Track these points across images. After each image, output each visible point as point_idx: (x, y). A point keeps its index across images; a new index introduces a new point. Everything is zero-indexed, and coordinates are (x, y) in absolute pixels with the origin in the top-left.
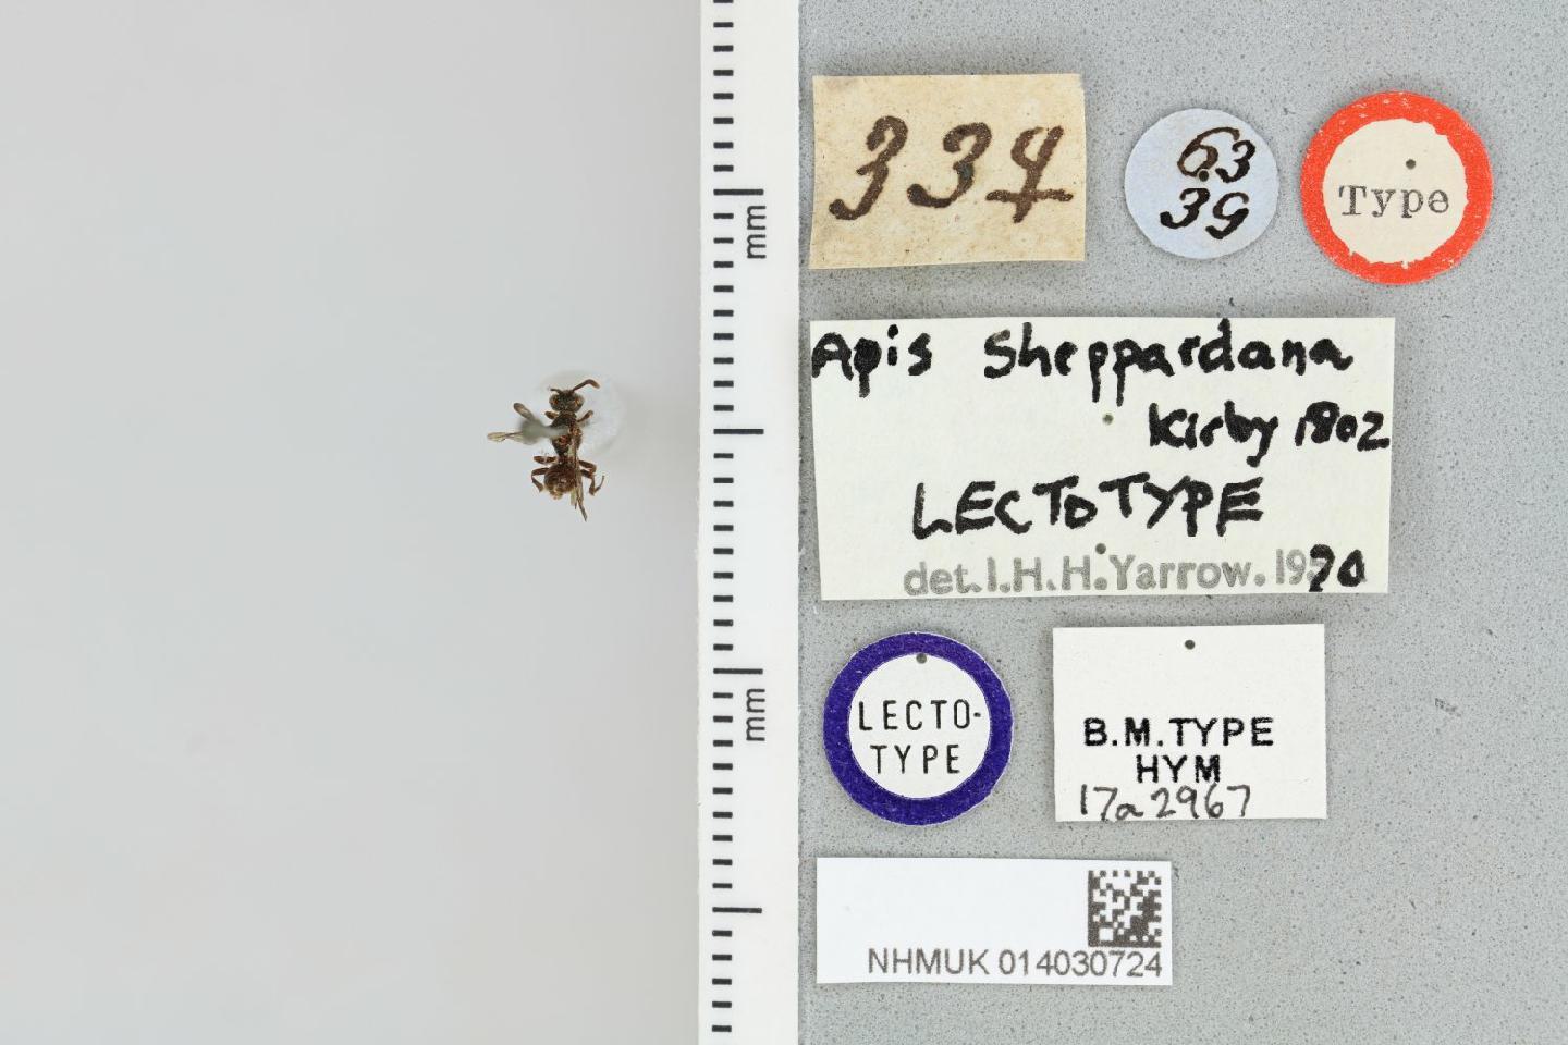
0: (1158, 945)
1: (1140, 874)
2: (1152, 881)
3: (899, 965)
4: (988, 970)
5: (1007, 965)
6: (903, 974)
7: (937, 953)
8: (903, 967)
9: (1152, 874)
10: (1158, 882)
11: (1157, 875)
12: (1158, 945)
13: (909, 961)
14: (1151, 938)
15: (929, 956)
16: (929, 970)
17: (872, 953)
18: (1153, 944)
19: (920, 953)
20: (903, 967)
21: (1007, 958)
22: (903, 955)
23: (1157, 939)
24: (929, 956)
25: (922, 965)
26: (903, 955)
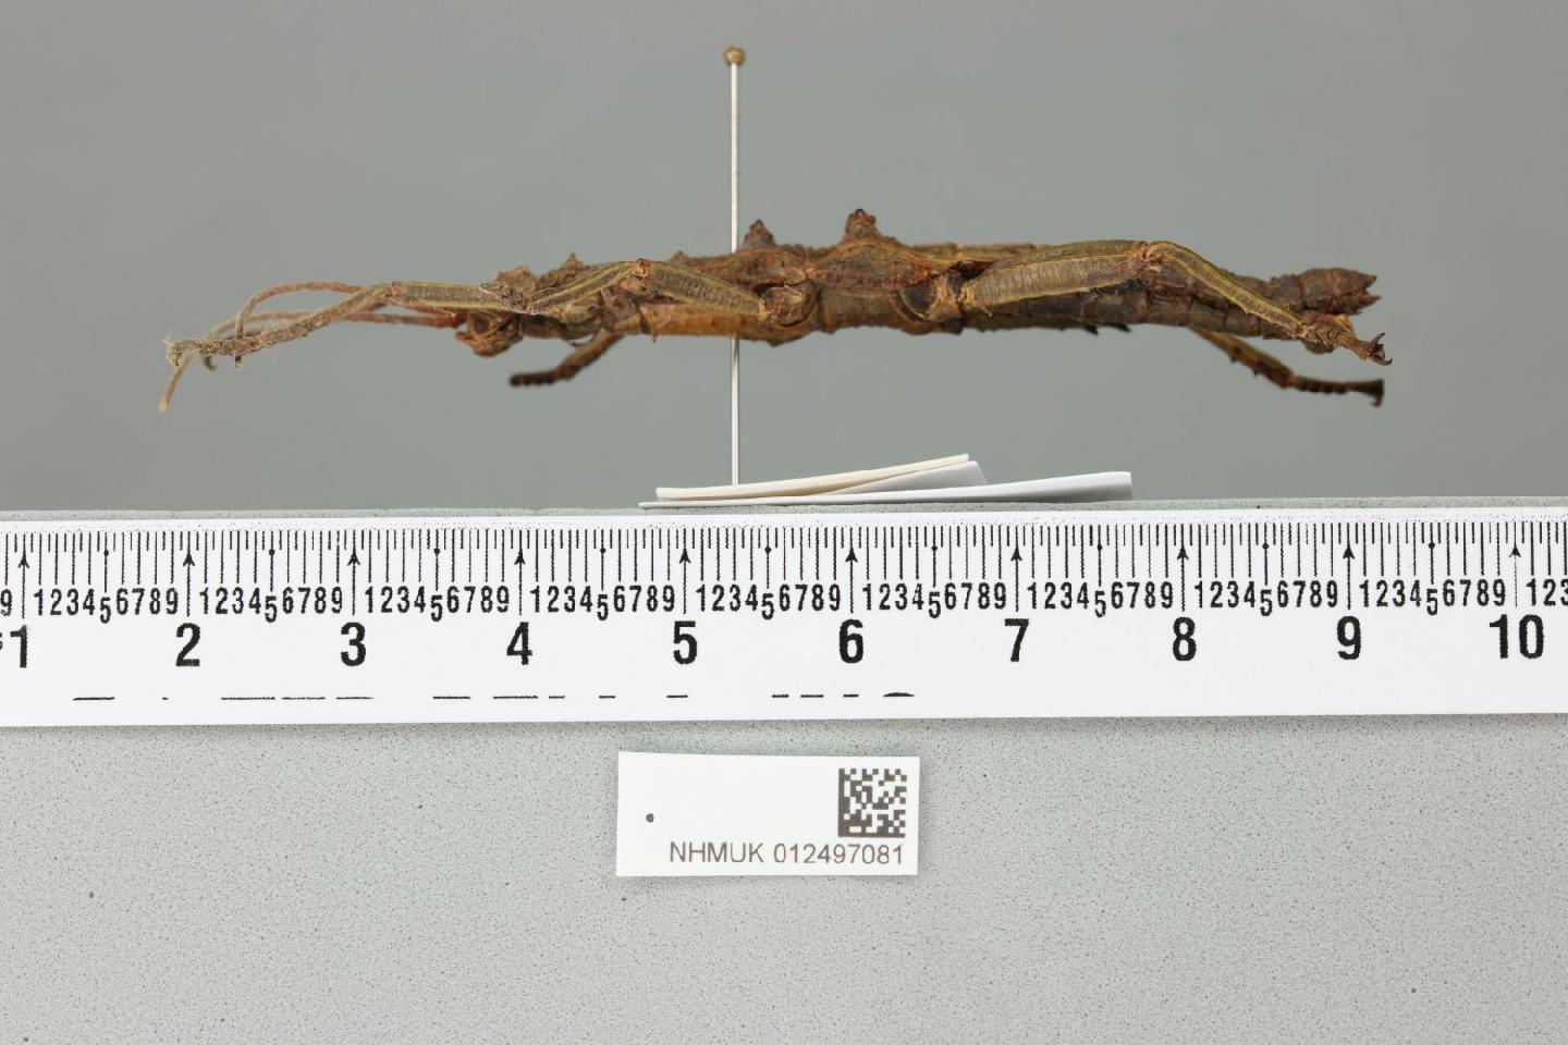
0: (903, 836)
1: (887, 771)
2: (898, 778)
3: (694, 854)
4: (763, 859)
5: (780, 857)
6: (698, 867)
7: (724, 846)
8: (697, 857)
9: (898, 772)
10: (904, 778)
11: (903, 773)
12: (903, 836)
13: (703, 852)
14: (896, 829)
15: (718, 850)
16: (717, 860)
17: (673, 845)
18: (897, 834)
19: (711, 845)
20: (697, 857)
21: (780, 849)
22: (697, 846)
23: (902, 830)
24: (718, 850)
25: (712, 856)
26: (697, 846)
